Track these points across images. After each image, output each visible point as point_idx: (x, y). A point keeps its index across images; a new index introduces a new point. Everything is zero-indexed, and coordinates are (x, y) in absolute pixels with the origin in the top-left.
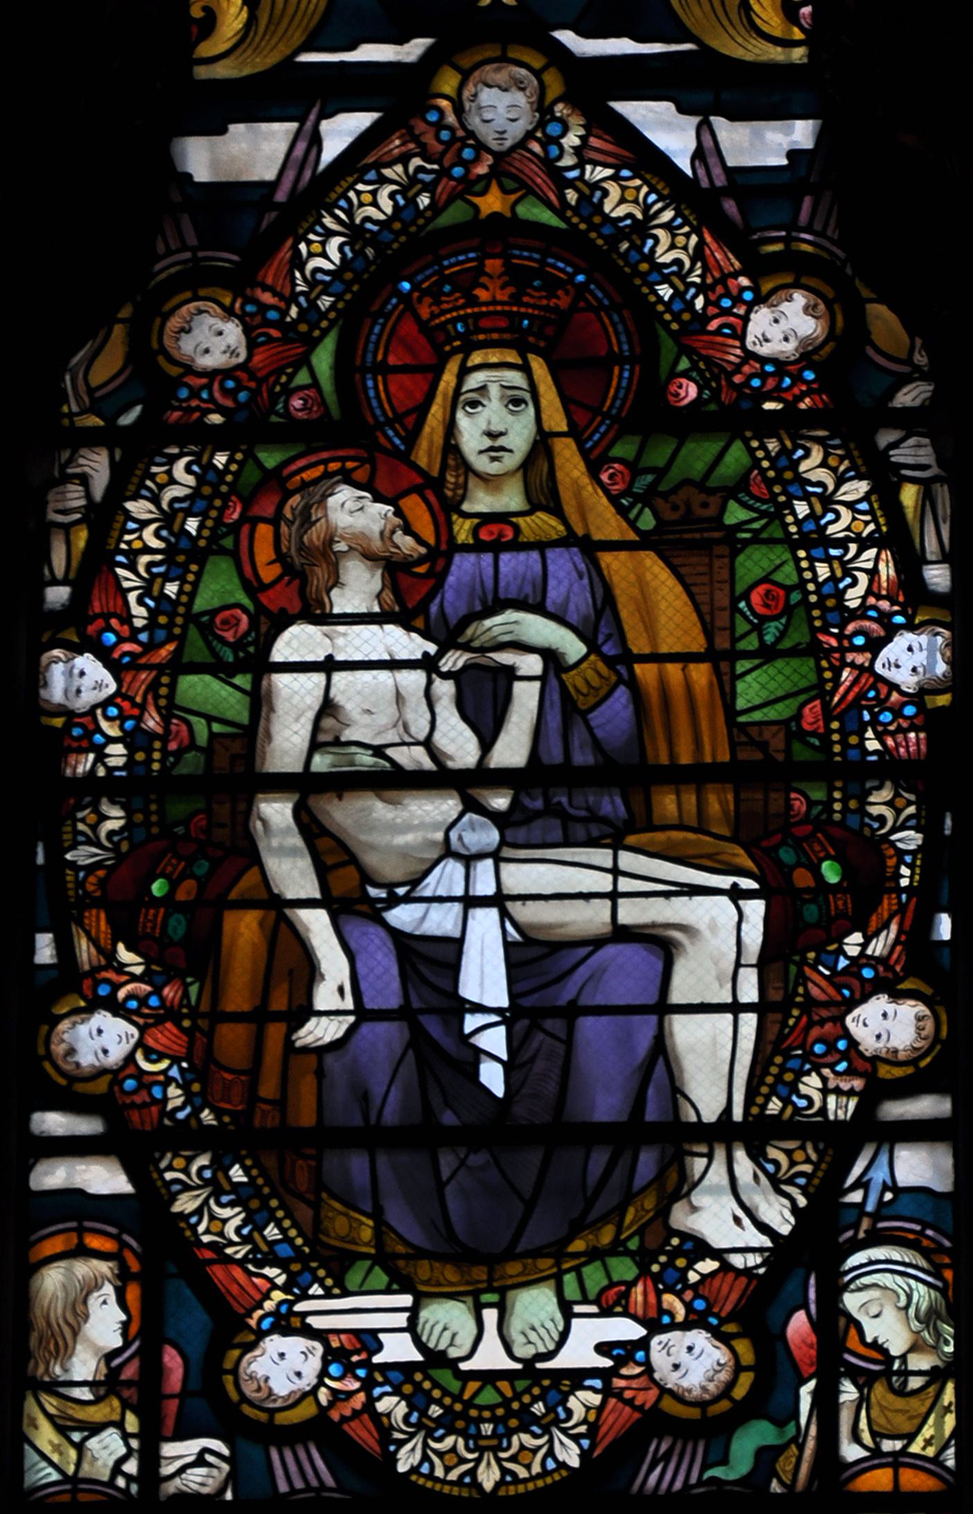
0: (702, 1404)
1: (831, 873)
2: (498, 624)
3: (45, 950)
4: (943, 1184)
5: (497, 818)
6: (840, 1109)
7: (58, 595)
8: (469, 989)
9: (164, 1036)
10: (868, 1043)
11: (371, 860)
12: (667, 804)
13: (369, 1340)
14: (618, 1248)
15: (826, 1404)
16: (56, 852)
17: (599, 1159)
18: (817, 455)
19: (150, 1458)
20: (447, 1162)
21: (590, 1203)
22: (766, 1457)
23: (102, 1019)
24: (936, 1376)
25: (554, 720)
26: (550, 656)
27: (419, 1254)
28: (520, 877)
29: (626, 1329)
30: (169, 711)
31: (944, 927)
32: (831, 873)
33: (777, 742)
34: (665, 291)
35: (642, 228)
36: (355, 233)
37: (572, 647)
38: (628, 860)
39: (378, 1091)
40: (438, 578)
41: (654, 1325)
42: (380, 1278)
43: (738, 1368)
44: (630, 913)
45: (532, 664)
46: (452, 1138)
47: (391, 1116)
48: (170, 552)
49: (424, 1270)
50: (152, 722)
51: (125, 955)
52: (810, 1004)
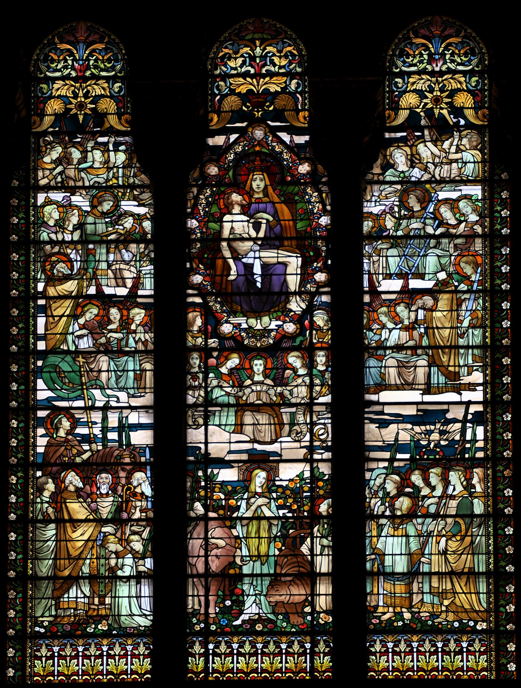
0: (292, 334)
1: (312, 254)
2: (259, 215)
3: (188, 265)
4: (329, 301)
5: (259, 245)
6: (313, 290)
7: (189, 210)
8: (255, 271)
9: (207, 278)
10: (318, 280)
11: (239, 251)
12: (286, 243)
13: (240, 324)
14: (278, 311)
15: (311, 334)
16: (189, 250)
17: (276, 297)
18: (309, 189)
19: (206, 342)
20: (252, 298)
21: (274, 304)
22: (301, 342)
23: (197, 276)
24: (328, 330)
25: (268, 230)
26: (267, 220)
27: (247, 312)
28: (263, 254)
29: (280, 323)
30: (207, 228)
31: (329, 262)
32: (312, 254)
33: (303, 233)
34: (285, 163)
35: (281, 153)
36: (236, 153)
37: (271, 219)
38: (280, 252)
39: (241, 287)
40: (250, 208)
41: (284, 322)
42: (242, 315)
43: (297, 329)
44: (280, 260)
45: (264, 221)
46: (253, 294)
47: (243, 290)
48: (207, 204)
49: (248, 314)
50: (204, 230)
51: (201, 266)
52: (308, 274)
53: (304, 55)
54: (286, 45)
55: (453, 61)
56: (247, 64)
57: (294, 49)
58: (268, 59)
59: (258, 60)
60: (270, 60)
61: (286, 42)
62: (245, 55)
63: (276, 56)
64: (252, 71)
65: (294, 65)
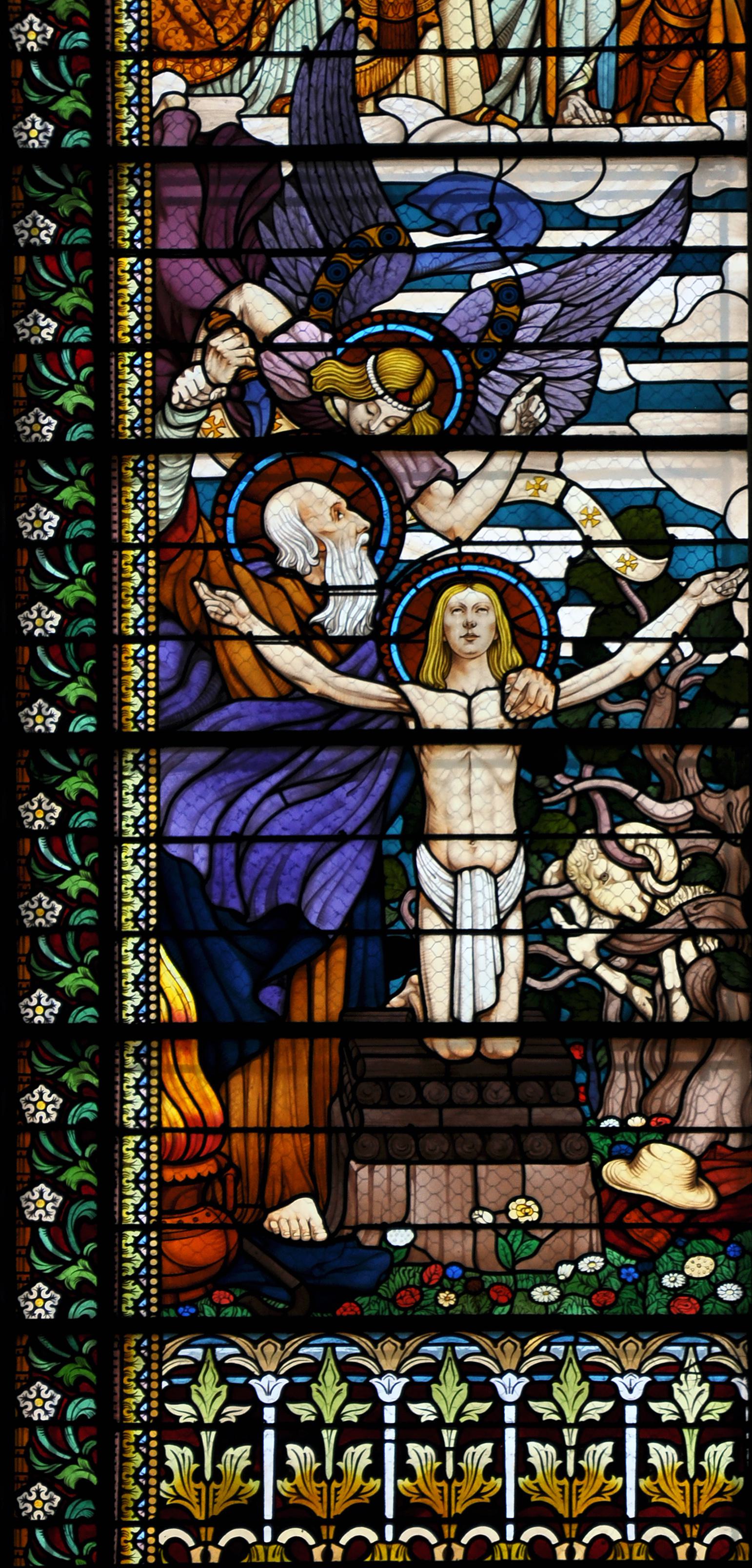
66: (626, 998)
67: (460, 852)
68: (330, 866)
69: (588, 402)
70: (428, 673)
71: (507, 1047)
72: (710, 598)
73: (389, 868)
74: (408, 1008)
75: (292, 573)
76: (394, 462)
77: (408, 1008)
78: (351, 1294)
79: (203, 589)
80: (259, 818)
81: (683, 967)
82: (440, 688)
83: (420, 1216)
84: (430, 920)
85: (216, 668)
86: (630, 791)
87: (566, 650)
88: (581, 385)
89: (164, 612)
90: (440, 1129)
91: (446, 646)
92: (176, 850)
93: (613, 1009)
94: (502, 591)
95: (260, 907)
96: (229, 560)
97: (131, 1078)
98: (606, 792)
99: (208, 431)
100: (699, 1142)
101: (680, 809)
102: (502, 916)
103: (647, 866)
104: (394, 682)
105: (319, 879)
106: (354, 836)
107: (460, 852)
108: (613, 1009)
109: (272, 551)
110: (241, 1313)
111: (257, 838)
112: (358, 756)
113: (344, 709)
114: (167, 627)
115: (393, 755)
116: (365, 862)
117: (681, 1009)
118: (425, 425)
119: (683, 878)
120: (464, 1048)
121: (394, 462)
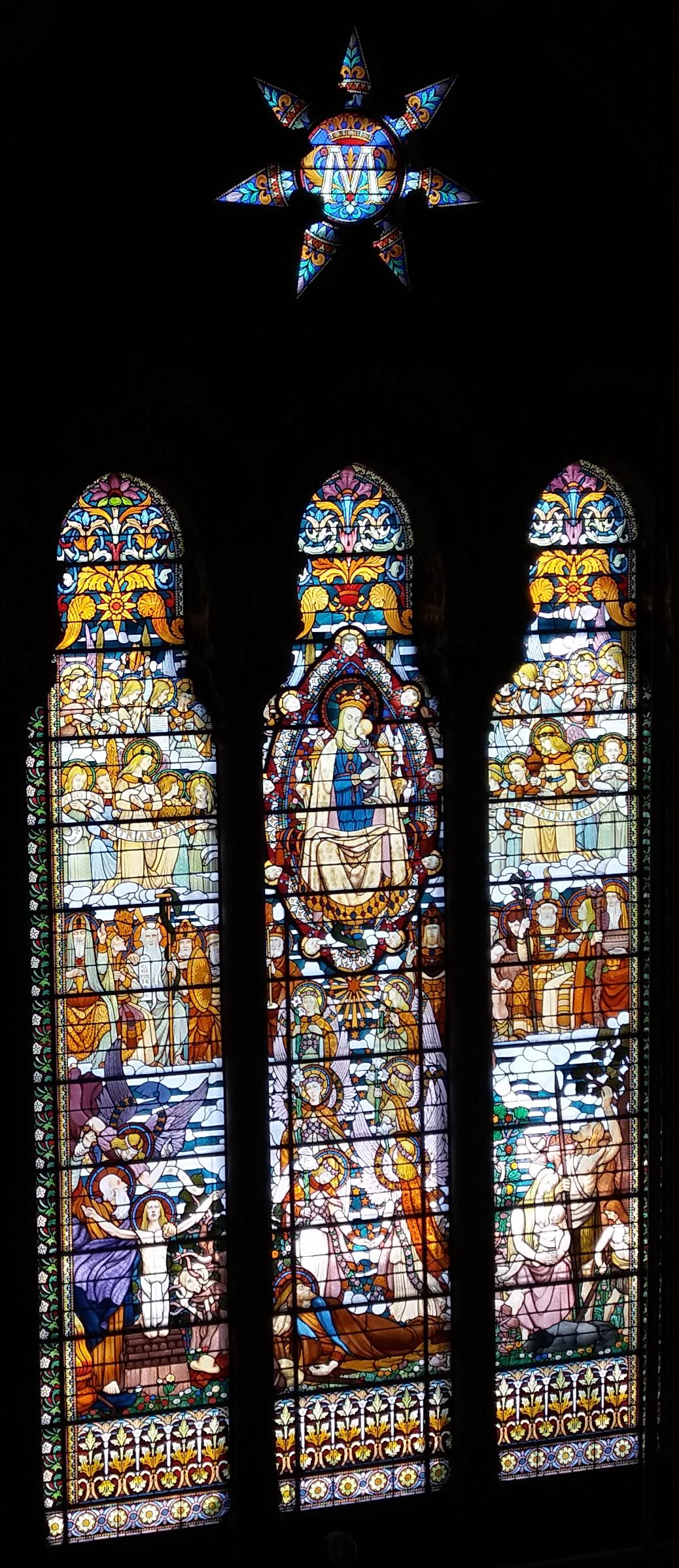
53: (177, 532)
54: (153, 515)
55: (368, 536)
56: (102, 547)
57: (163, 522)
58: (129, 537)
59: (116, 540)
60: (132, 539)
61: (153, 512)
62: (98, 531)
63: (139, 533)
64: (109, 557)
65: (164, 547)
66: (196, 1315)
67: (152, 1278)
68: (118, 1285)
69: (183, 1145)
70: (143, 1227)
71: (165, 1332)
72: (216, 1198)
73: (134, 1283)
74: (140, 1324)
75: (107, 1201)
76: (132, 1166)
77: (140, 1324)
78: (125, 1408)
79: (83, 1207)
80: (100, 1273)
81: (210, 1305)
82: (146, 1230)
83: (144, 1383)
84: (145, 1298)
85: (88, 1231)
86: (195, 1255)
87: (179, 1217)
88: (181, 1140)
89: (74, 1216)
90: (149, 1358)
91: (148, 1219)
92: (78, 1285)
93: (193, 1318)
94: (161, 1200)
95: (100, 1300)
96: (90, 1198)
97: (67, 1353)
98: (190, 1256)
99: (84, 1163)
100: (215, 1354)
101: (209, 1259)
102: (163, 1295)
103: (200, 1276)
104: (134, 1230)
105: (115, 1289)
106: (124, 1277)
107: (152, 1278)
108: (193, 1318)
109: (101, 1195)
110: (98, 1416)
111: (99, 1280)
112: (125, 1253)
113: (122, 1240)
114: (74, 1219)
115: (134, 1252)
116: (128, 1284)
117: (210, 1317)
118: (142, 1156)
119: (210, 1279)
120: (154, 1334)
121: (132, 1166)
